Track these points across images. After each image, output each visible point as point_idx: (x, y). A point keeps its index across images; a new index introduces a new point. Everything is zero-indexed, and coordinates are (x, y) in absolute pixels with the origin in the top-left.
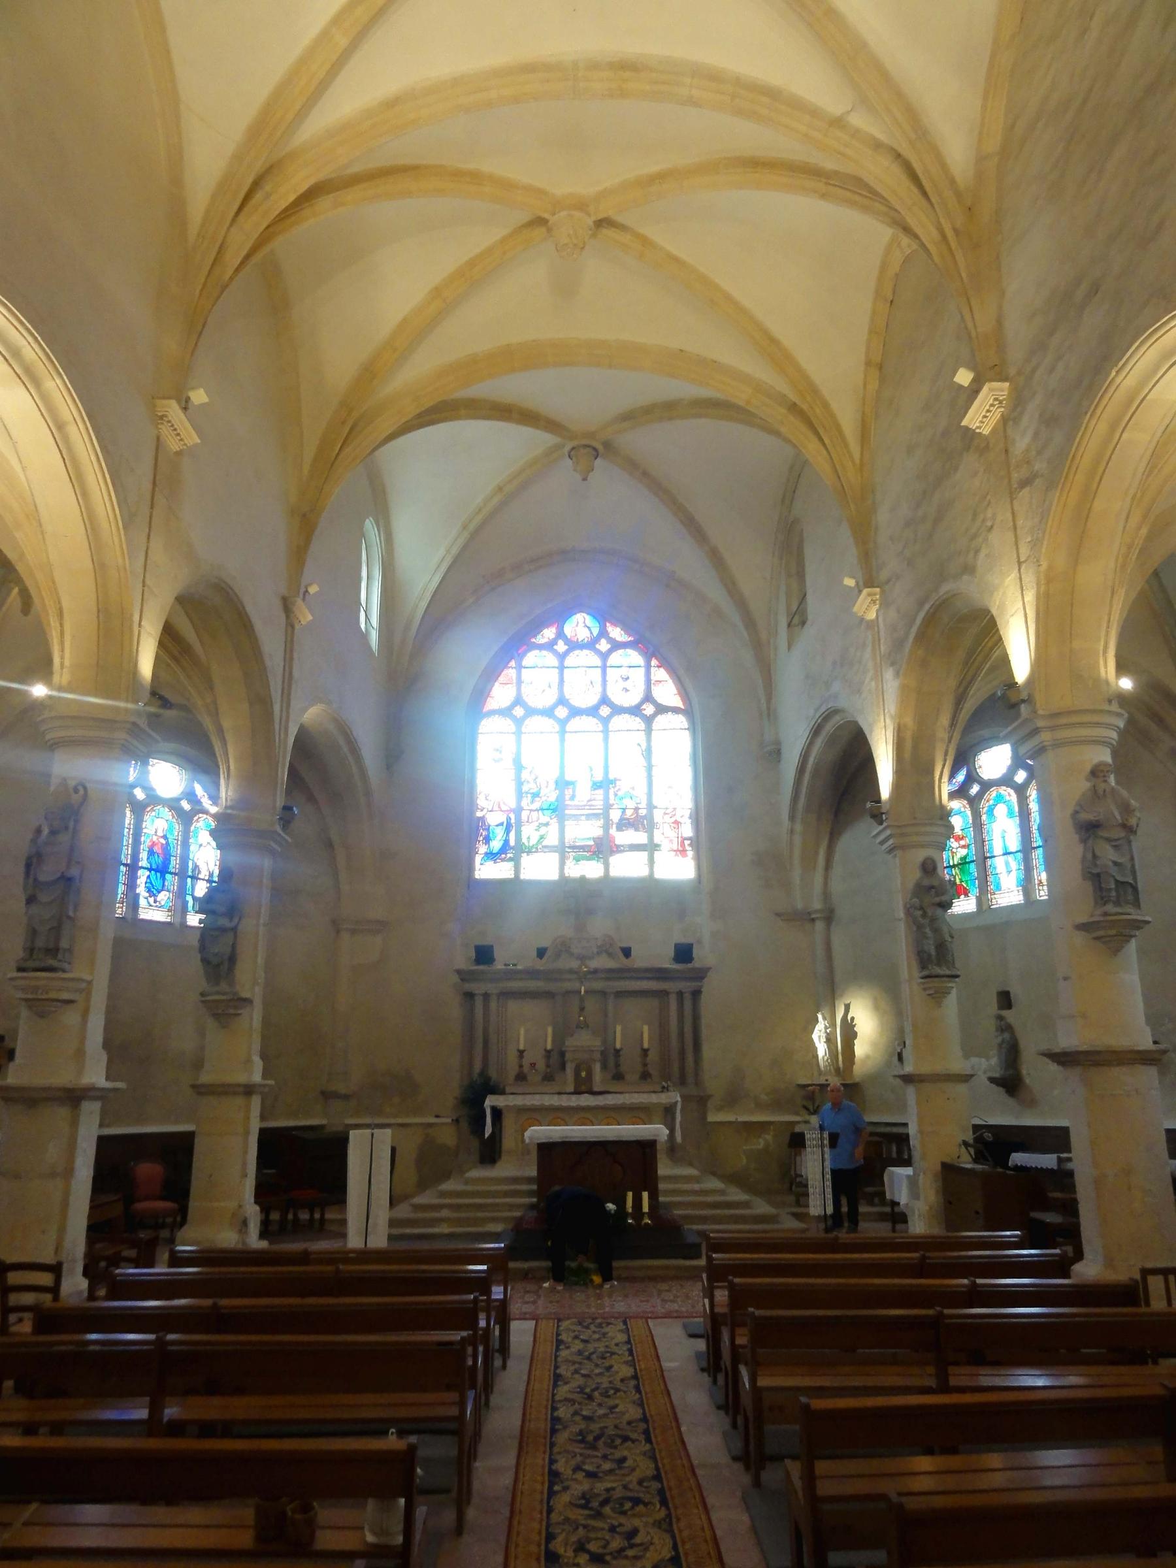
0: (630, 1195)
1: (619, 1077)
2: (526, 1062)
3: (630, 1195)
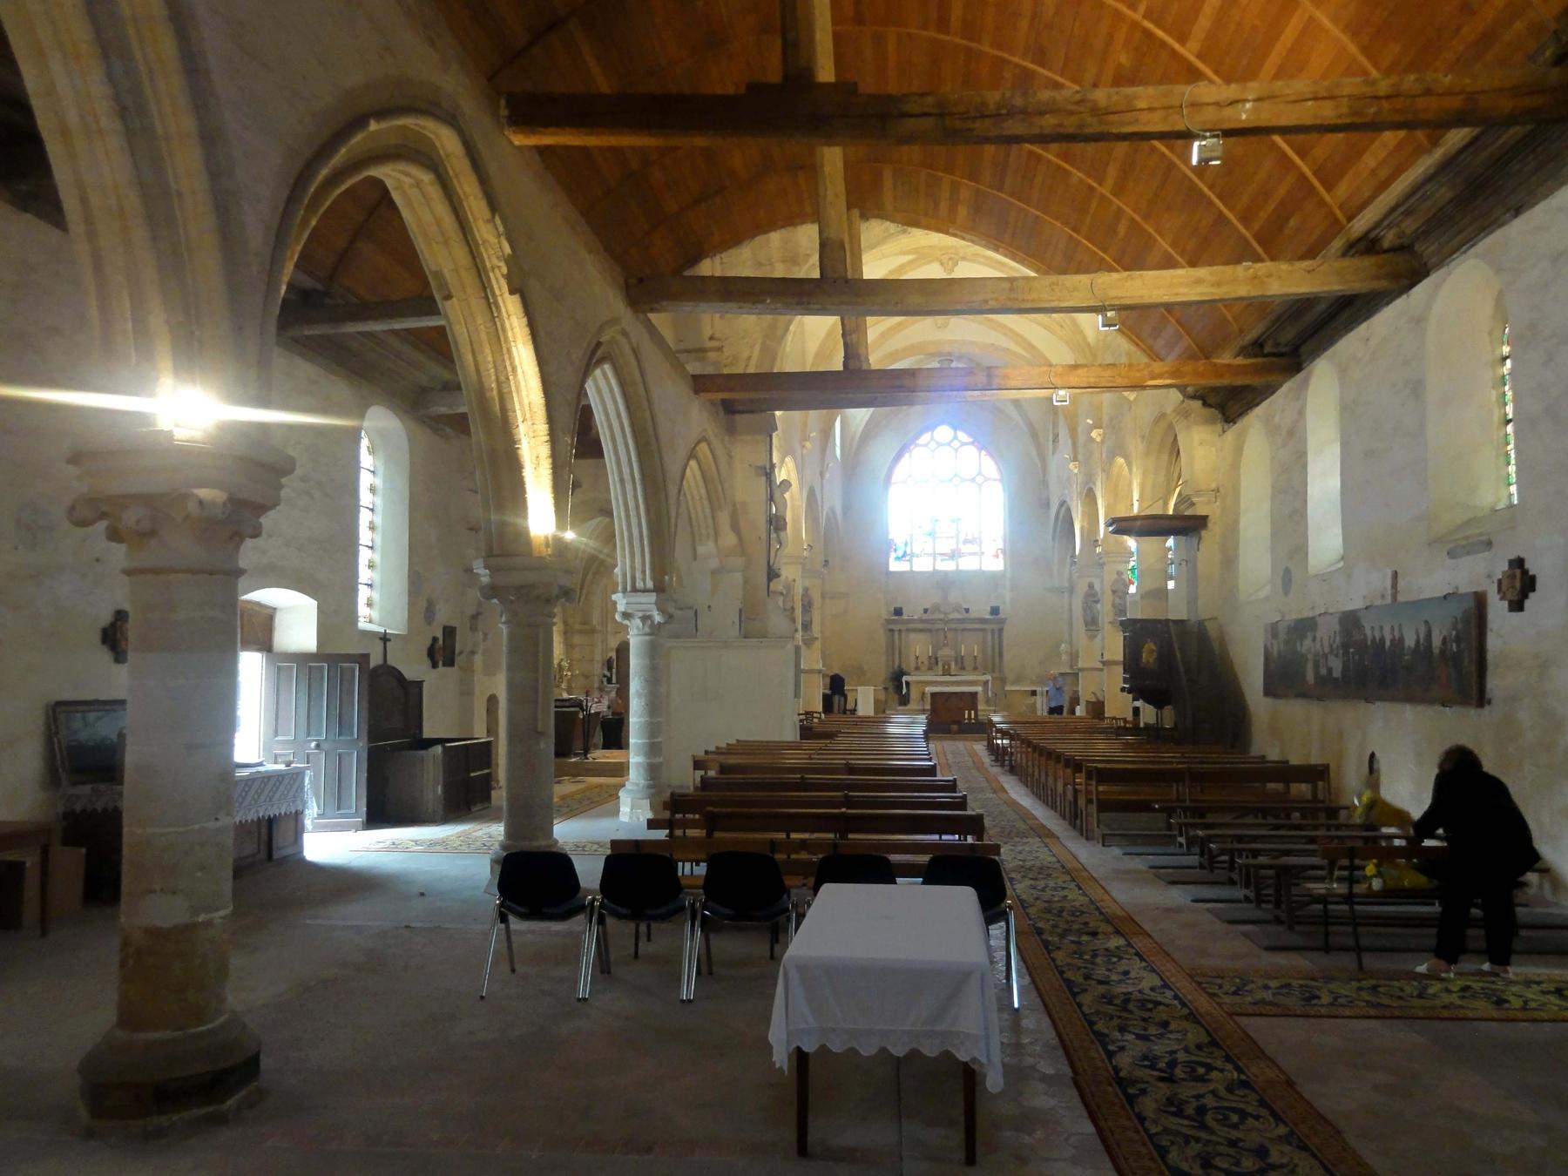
0: (967, 712)
1: (963, 668)
2: (920, 661)
3: (967, 712)
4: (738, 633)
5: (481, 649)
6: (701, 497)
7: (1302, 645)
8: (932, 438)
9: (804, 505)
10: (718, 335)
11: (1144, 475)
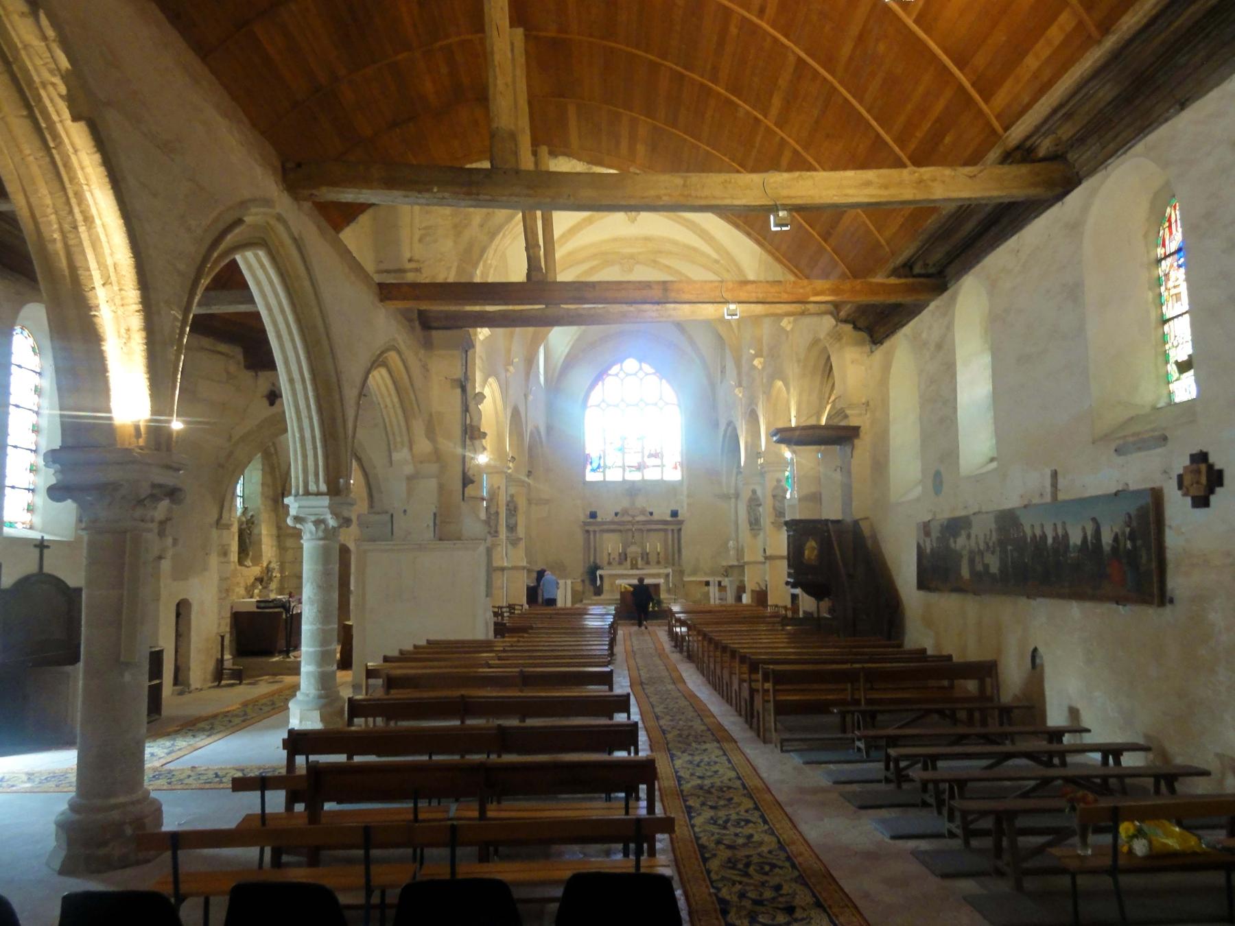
1: (648, 563)
2: (612, 557)
4: (432, 535)
5: (170, 554)
6: (394, 406)
7: (955, 542)
8: (621, 369)
9: (508, 422)
10: (416, 257)
11: (800, 394)
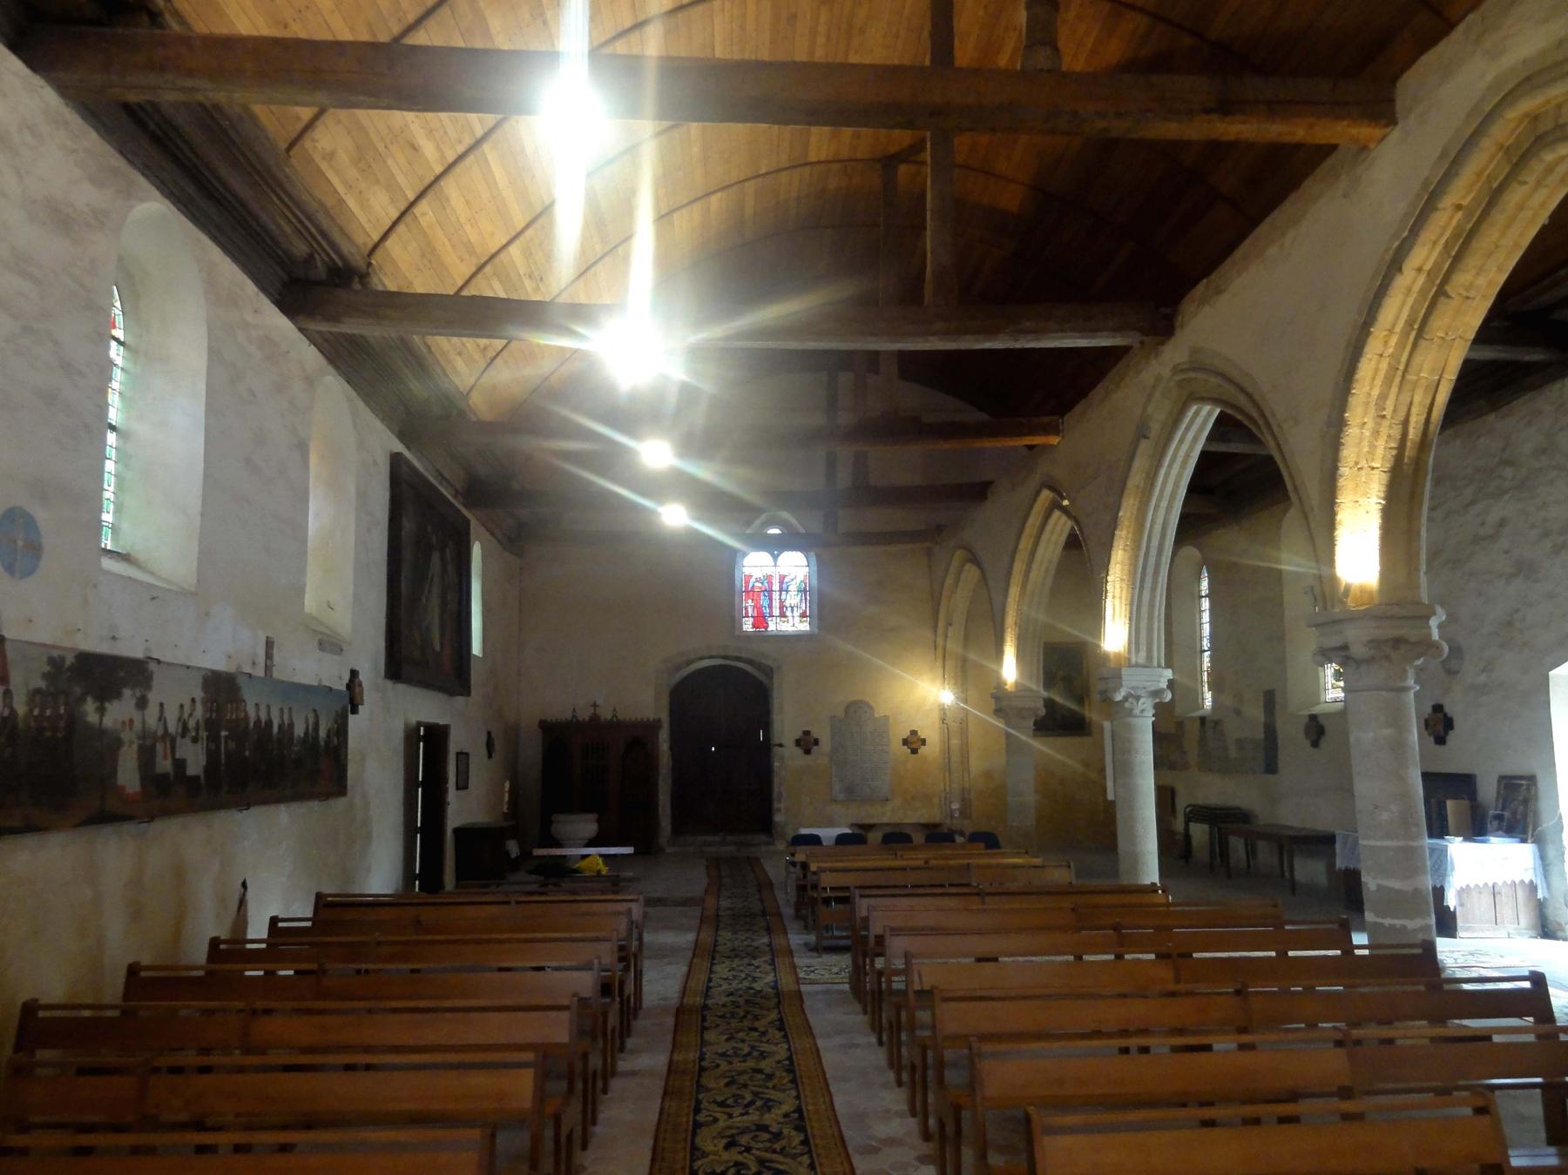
7: (101, 711)
